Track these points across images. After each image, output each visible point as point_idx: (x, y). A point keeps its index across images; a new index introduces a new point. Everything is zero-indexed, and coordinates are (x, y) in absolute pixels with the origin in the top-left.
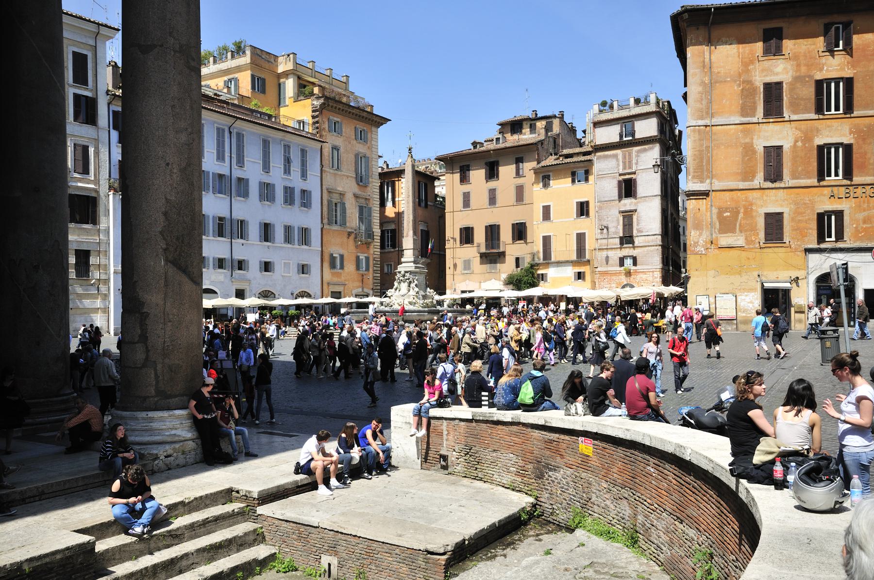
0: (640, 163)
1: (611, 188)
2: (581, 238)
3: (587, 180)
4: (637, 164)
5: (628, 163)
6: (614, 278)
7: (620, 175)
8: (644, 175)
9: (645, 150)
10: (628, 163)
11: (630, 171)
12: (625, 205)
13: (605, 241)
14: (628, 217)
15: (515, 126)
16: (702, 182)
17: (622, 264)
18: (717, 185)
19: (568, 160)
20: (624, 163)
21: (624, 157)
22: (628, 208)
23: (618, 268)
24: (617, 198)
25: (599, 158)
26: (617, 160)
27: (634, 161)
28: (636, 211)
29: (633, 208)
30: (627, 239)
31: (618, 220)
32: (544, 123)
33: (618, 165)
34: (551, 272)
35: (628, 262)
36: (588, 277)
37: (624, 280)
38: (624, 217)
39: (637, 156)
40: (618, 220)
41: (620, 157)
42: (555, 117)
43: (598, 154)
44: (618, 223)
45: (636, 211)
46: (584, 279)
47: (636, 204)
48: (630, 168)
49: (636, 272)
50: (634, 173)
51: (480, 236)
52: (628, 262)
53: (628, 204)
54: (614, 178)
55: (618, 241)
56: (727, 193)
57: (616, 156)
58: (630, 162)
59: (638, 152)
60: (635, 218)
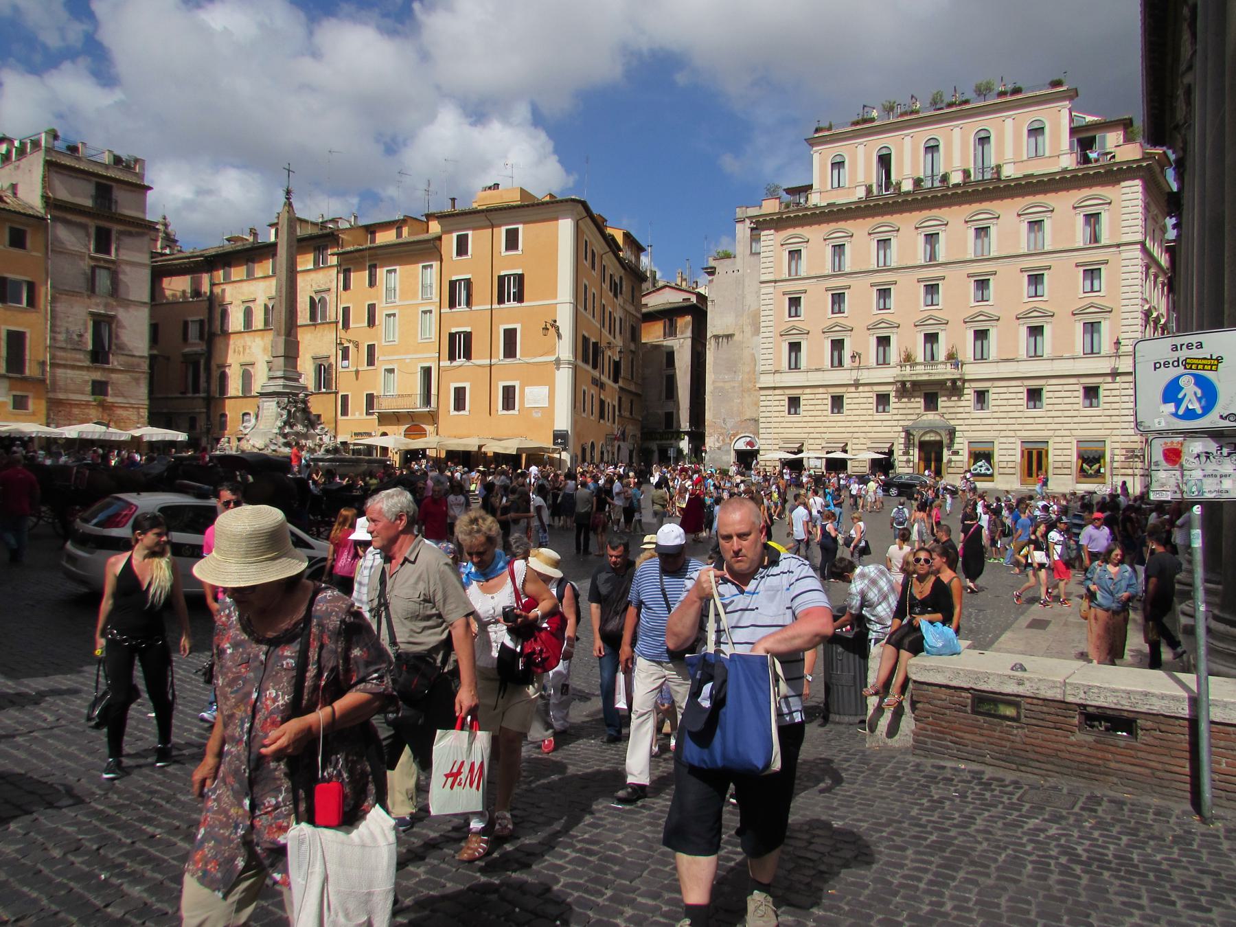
0: (122, 251)
2: (16, 341)
5: (103, 243)
7: (92, 258)
8: (127, 269)
9: (130, 234)
10: (103, 243)
12: (97, 305)
14: (102, 324)
28: (113, 318)
30: (99, 355)
31: (86, 324)
38: (95, 323)
39: (118, 239)
40: (86, 324)
41: (92, 231)
44: (86, 329)
50: (113, 262)
57: (84, 227)
59: (121, 233)
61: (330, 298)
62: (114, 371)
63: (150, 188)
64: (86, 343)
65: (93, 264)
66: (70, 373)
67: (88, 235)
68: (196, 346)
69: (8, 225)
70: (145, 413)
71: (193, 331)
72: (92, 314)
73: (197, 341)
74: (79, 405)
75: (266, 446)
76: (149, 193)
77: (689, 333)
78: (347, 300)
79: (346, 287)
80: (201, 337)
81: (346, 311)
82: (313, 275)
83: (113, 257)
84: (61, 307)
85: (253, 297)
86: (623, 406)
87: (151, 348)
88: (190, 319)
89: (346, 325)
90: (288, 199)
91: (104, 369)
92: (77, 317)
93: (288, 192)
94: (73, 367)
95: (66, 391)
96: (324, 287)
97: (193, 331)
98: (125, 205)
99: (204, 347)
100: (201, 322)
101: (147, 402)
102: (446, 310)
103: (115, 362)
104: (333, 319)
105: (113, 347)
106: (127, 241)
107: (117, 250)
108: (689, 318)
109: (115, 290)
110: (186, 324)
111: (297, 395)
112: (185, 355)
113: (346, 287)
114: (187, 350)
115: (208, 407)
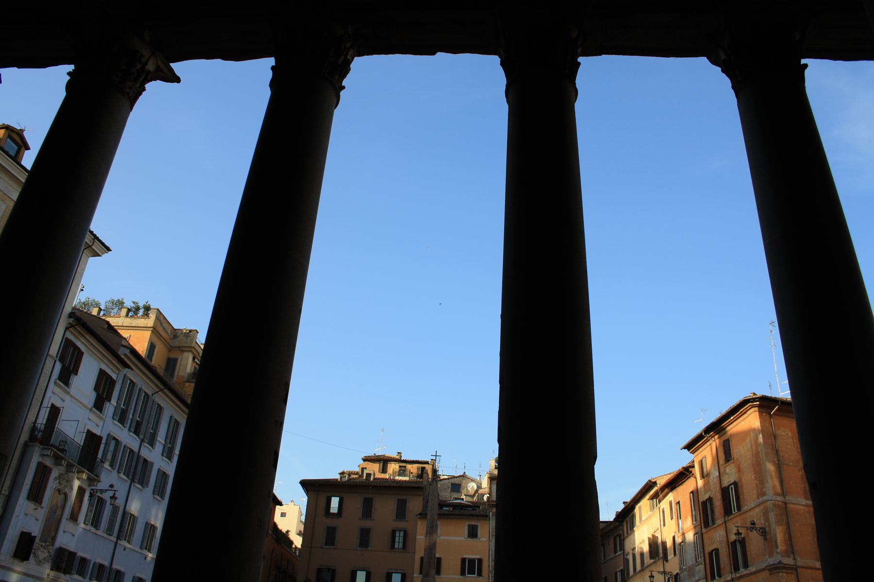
15: (384, 461)
16: (788, 557)
18: (800, 562)
42: (427, 463)
56: (809, 572)
69: (467, 523)
79: (664, 525)
110: (616, 573)
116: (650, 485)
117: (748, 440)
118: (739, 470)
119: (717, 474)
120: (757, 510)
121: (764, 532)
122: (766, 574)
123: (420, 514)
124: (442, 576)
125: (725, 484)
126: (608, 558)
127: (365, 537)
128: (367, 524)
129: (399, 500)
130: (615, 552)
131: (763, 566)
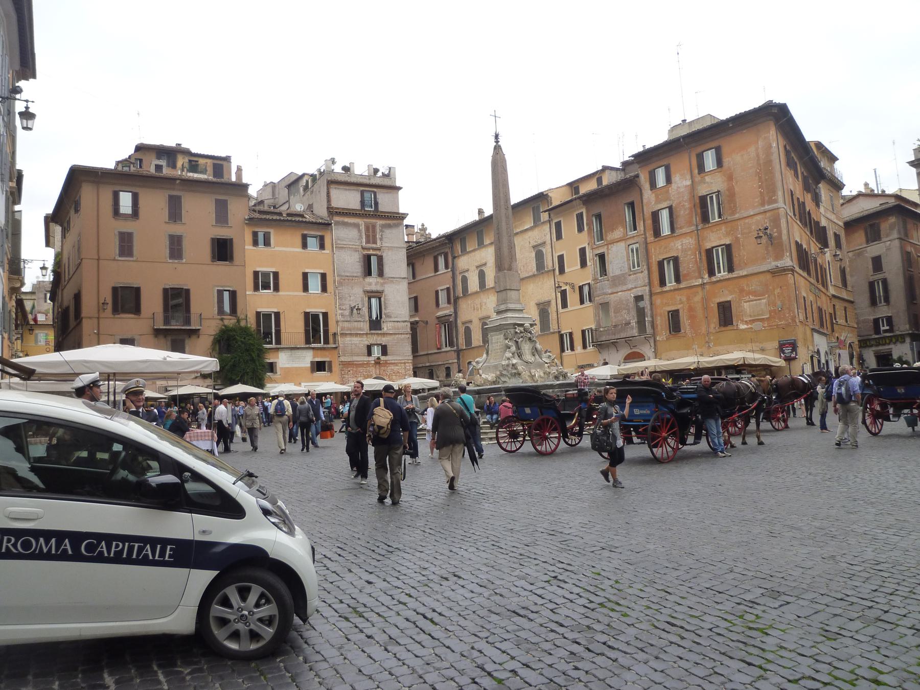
1: (351, 262)
3: (322, 247)
4: (381, 239)
5: (371, 236)
6: (361, 369)
7: (363, 248)
9: (389, 226)
10: (371, 236)
11: (374, 246)
12: (370, 284)
13: (346, 325)
17: (369, 354)
19: (264, 217)
20: (367, 236)
21: (367, 229)
22: (374, 288)
23: (366, 359)
24: (359, 274)
25: (337, 223)
26: (359, 231)
27: (378, 236)
28: (381, 292)
29: (379, 288)
30: (375, 325)
32: (209, 161)
33: (361, 236)
34: (283, 360)
35: (376, 352)
36: (336, 367)
37: (373, 371)
39: (381, 231)
40: (362, 300)
41: (363, 228)
43: (337, 218)
45: (381, 292)
46: (330, 370)
47: (382, 284)
48: (375, 242)
49: (386, 363)
51: (152, 303)
52: (376, 352)
53: (373, 283)
54: (356, 250)
55: (366, 326)
57: (357, 226)
58: (374, 236)
59: (383, 226)
60: (382, 299)
61: (547, 250)
62: (384, 334)
63: (400, 188)
64: (364, 316)
65: (366, 252)
66: (356, 340)
67: (359, 231)
68: (446, 310)
70: (410, 367)
71: (443, 297)
72: (366, 292)
73: (446, 305)
74: (362, 365)
75: (497, 377)
76: (400, 192)
77: (895, 235)
78: (561, 248)
79: (559, 236)
80: (449, 302)
81: (561, 258)
82: (530, 233)
83: (379, 245)
84: (345, 290)
85: (484, 262)
86: (838, 313)
87: (411, 316)
88: (439, 288)
89: (562, 271)
90: (497, 142)
91: (378, 334)
92: (355, 295)
93: (497, 136)
94: (357, 335)
95: (352, 354)
96: (539, 242)
97: (443, 297)
98: (385, 202)
99: (452, 310)
100: (448, 289)
101: (411, 358)
102: (651, 238)
103: (386, 327)
104: (550, 268)
105: (383, 316)
106: (387, 232)
107: (381, 239)
108: (892, 219)
109: (381, 273)
110: (437, 292)
111: (522, 325)
112: (438, 318)
113: (559, 236)
114: (440, 313)
115: (458, 359)
116: (541, 197)
117: (752, 150)
118: (730, 178)
119: (689, 183)
120: (758, 218)
121: (770, 237)
122: (769, 276)
123: (250, 219)
124: (280, 293)
125: (703, 191)
126: (417, 279)
127: (176, 247)
128: (176, 229)
129: (217, 200)
130: (436, 269)
131: (766, 269)
